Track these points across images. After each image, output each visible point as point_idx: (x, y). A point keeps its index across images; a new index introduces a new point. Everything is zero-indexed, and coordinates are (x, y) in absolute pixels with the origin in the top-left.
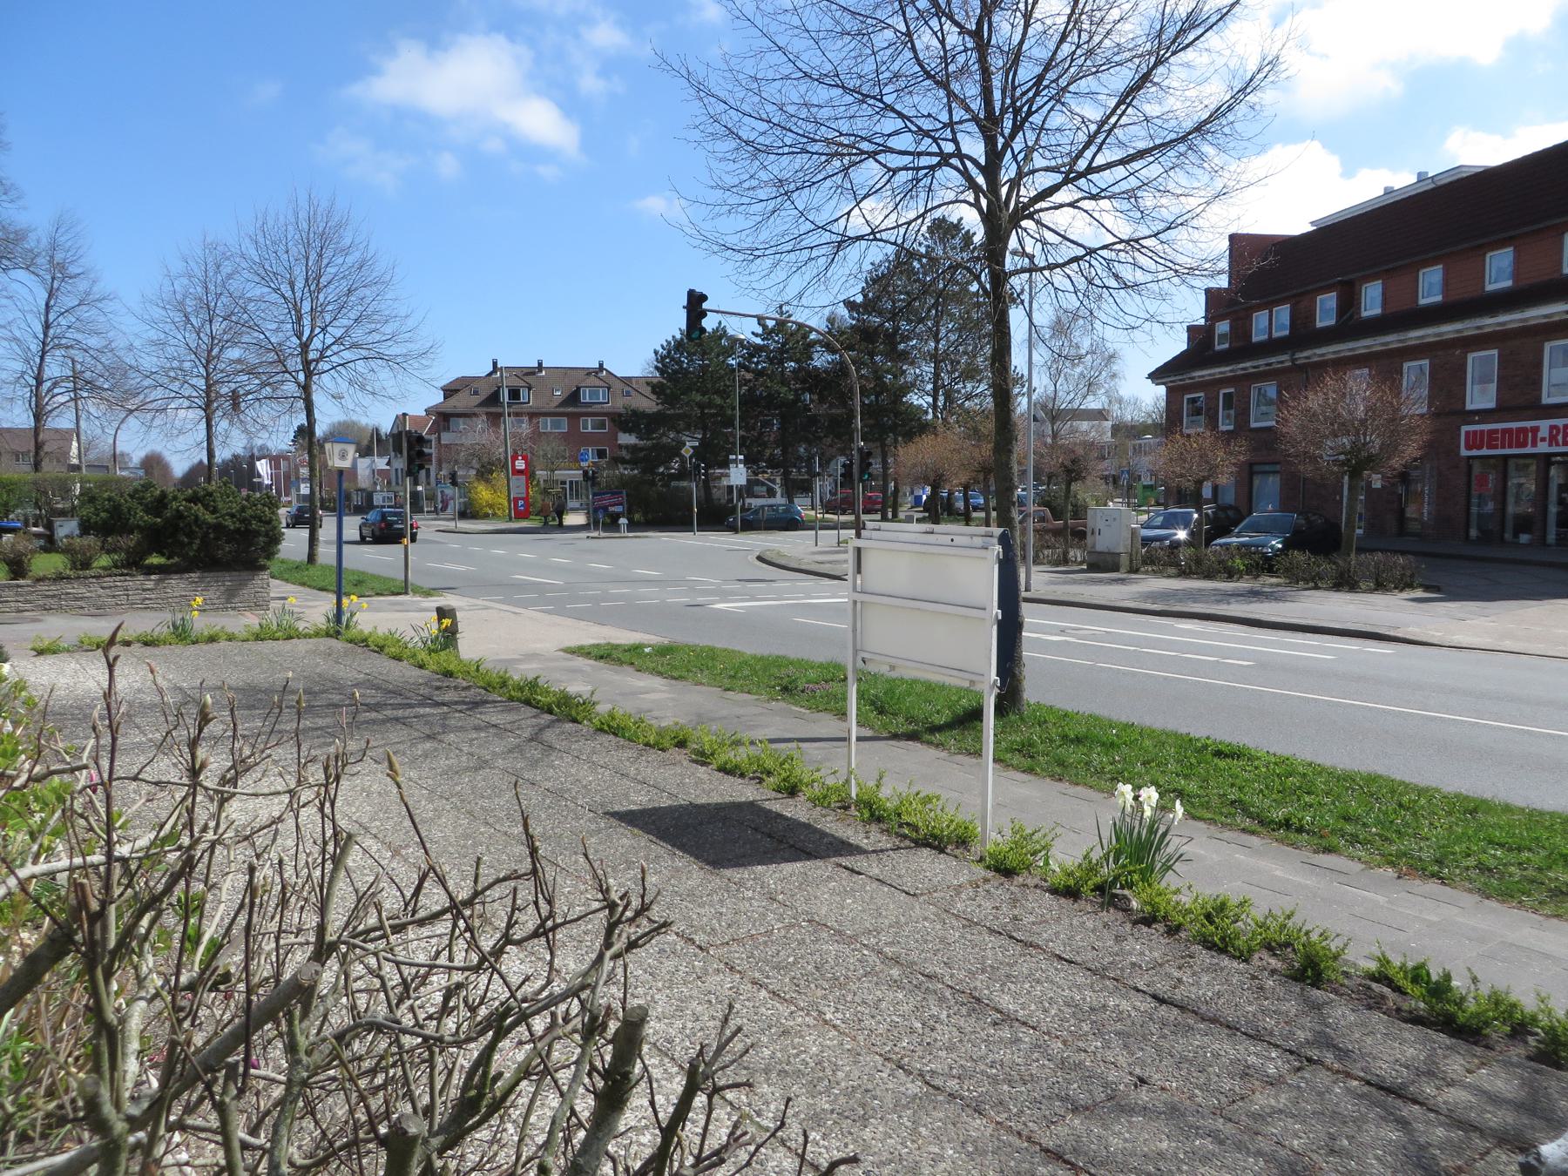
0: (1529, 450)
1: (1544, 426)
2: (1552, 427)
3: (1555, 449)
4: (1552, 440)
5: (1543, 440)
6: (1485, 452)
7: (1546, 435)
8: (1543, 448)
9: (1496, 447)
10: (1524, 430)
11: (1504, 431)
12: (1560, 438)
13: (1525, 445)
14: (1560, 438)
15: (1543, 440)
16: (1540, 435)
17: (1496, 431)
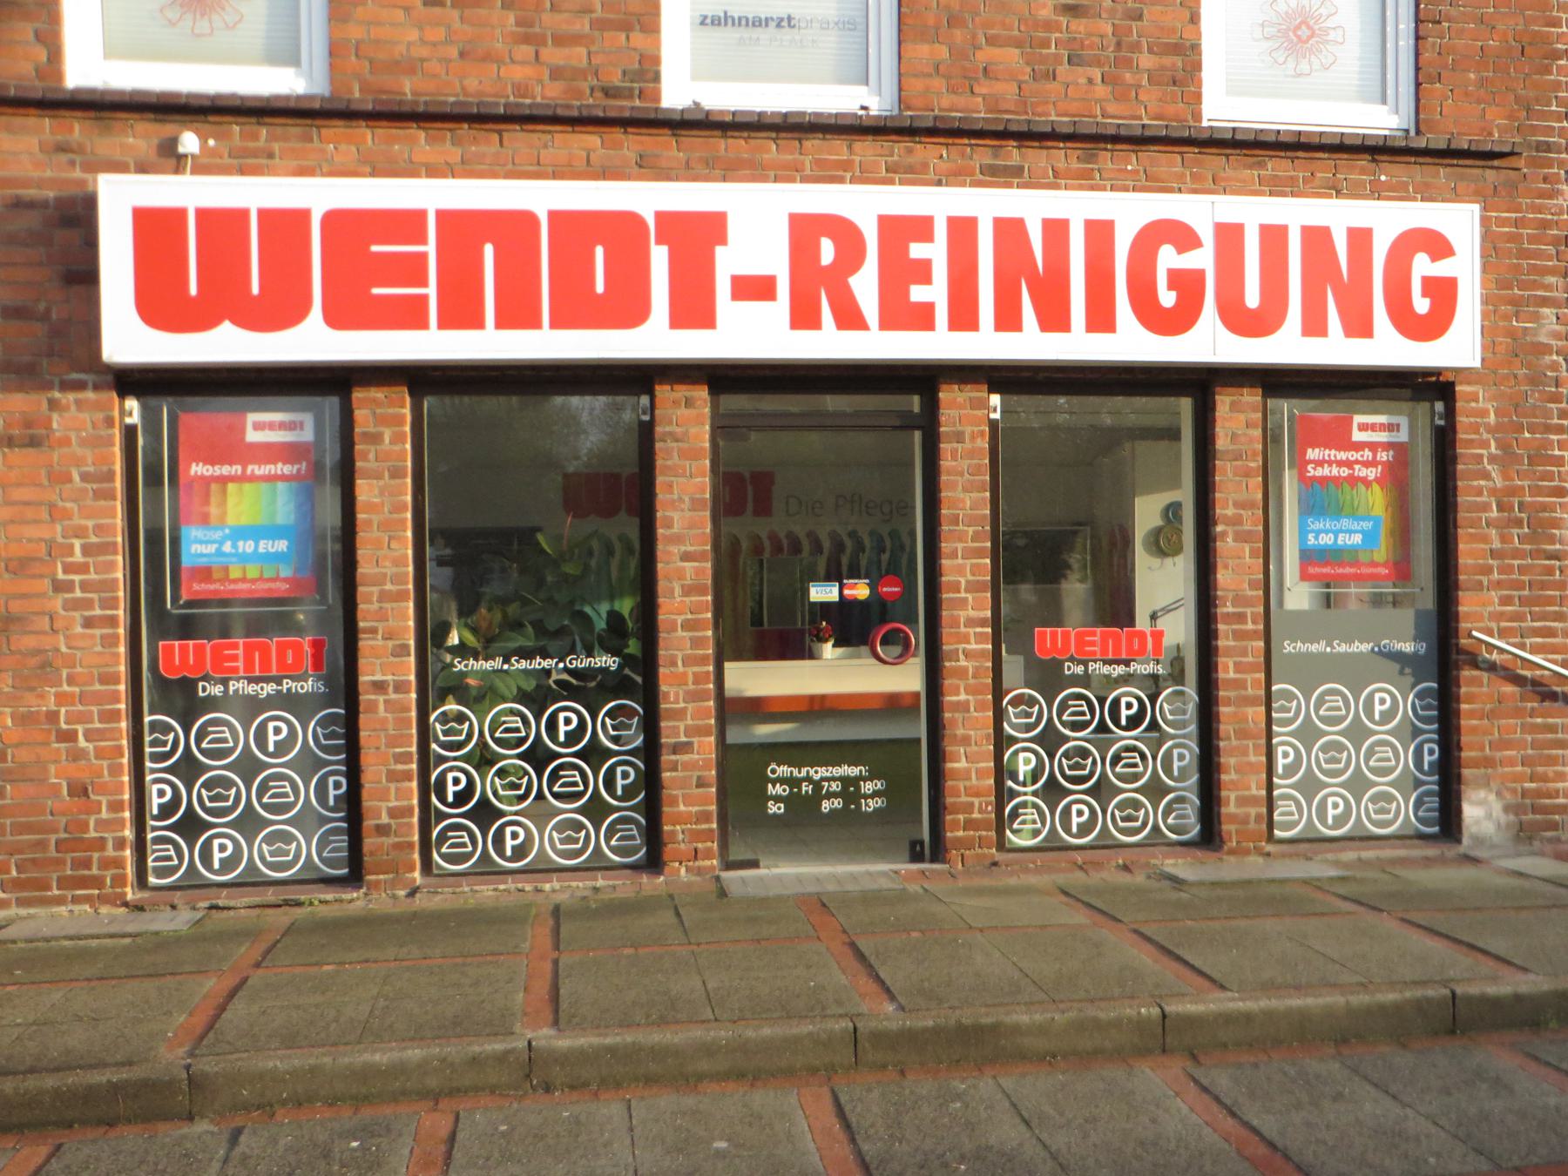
0: (653, 339)
1: (757, 220)
2: (805, 230)
3: (829, 344)
4: (814, 290)
5: (754, 288)
6: (312, 341)
7: (775, 261)
8: (753, 333)
9: (410, 316)
10: (623, 232)
11: (462, 229)
12: (865, 286)
13: (631, 312)
14: (865, 286)
15: (754, 288)
16: (729, 262)
17: (408, 223)
